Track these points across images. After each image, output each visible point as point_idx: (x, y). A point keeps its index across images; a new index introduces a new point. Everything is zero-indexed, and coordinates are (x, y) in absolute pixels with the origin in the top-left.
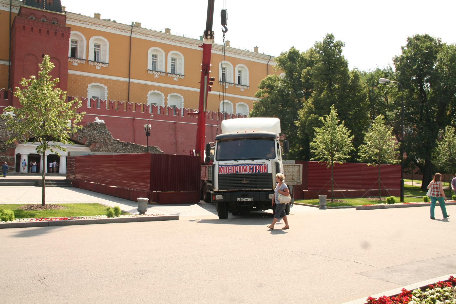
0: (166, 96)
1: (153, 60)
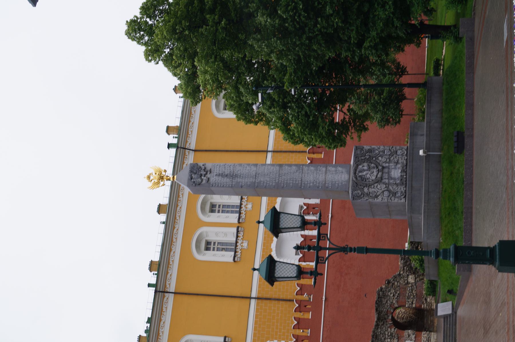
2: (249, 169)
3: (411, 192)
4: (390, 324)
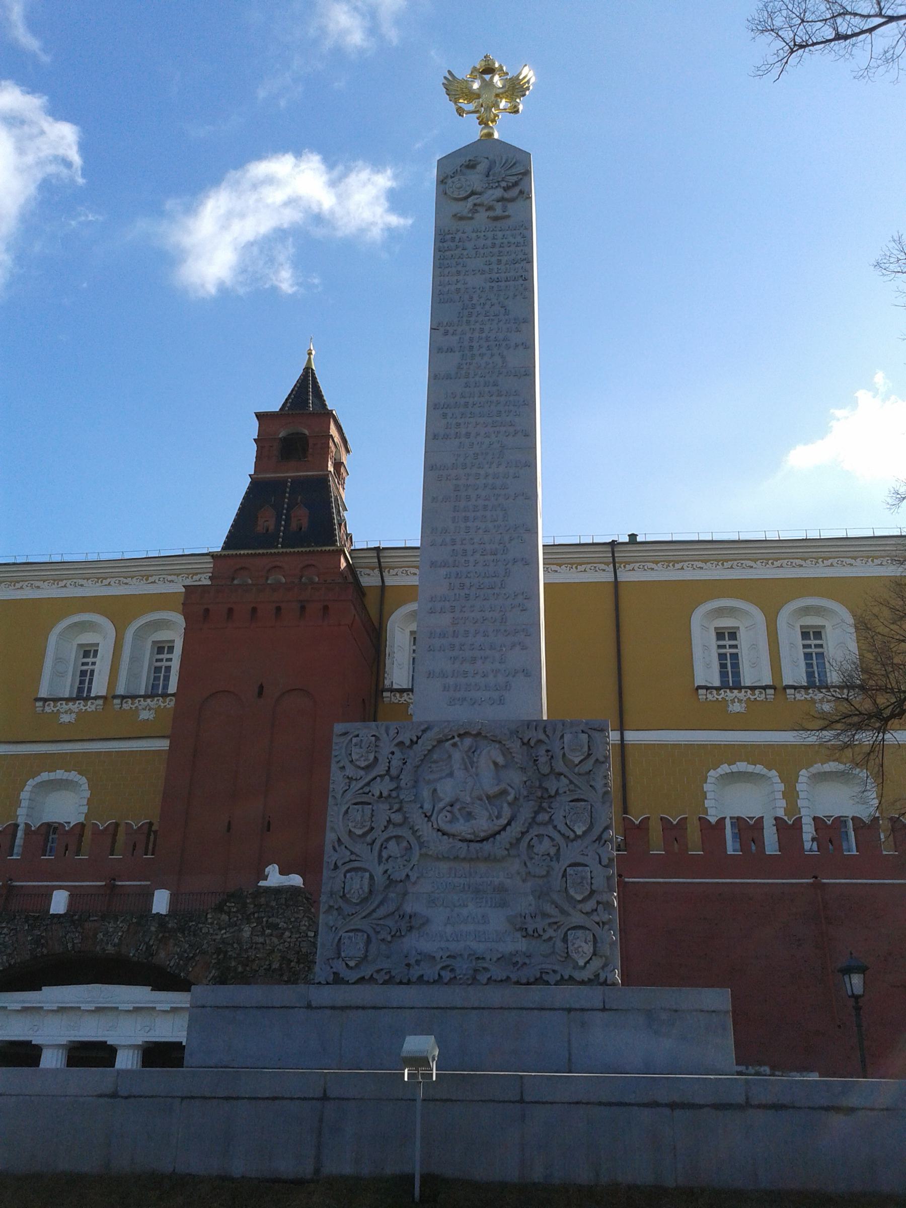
0: (790, 782)
1: (723, 651)
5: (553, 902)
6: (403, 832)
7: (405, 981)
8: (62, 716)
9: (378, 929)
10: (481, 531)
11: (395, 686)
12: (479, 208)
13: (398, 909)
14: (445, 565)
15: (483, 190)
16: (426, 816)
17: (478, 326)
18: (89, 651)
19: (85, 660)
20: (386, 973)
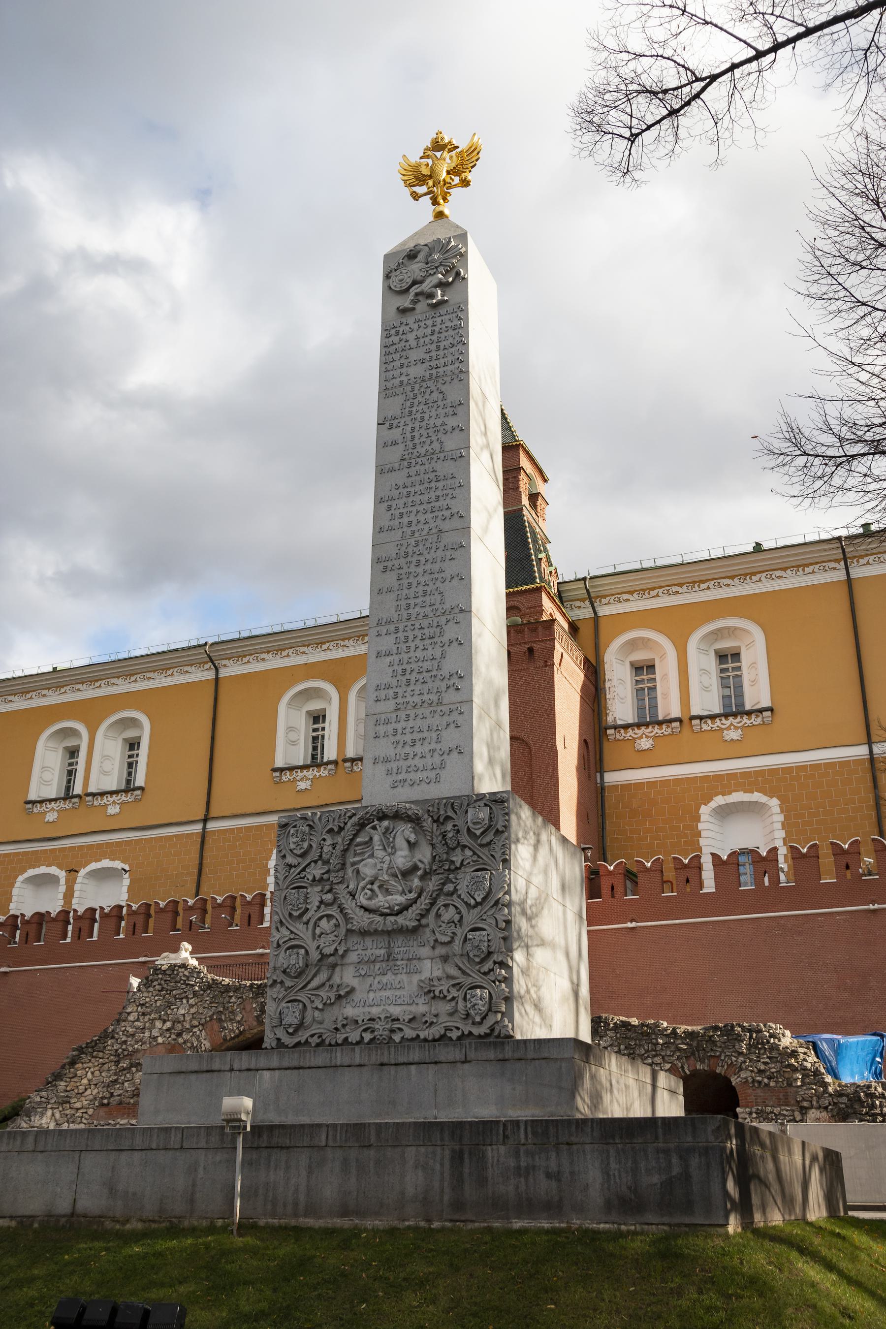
2: (449, 428)
3: (232, 1070)
4: (682, 1067)
5: (457, 966)
6: (334, 911)
7: (333, 1042)
8: (300, 783)
9: (313, 998)
10: (420, 617)
11: (619, 722)
12: (420, 298)
13: (328, 980)
14: (389, 654)
15: (422, 278)
16: (351, 895)
17: (418, 416)
18: (318, 718)
19: (316, 726)
20: (319, 1037)
